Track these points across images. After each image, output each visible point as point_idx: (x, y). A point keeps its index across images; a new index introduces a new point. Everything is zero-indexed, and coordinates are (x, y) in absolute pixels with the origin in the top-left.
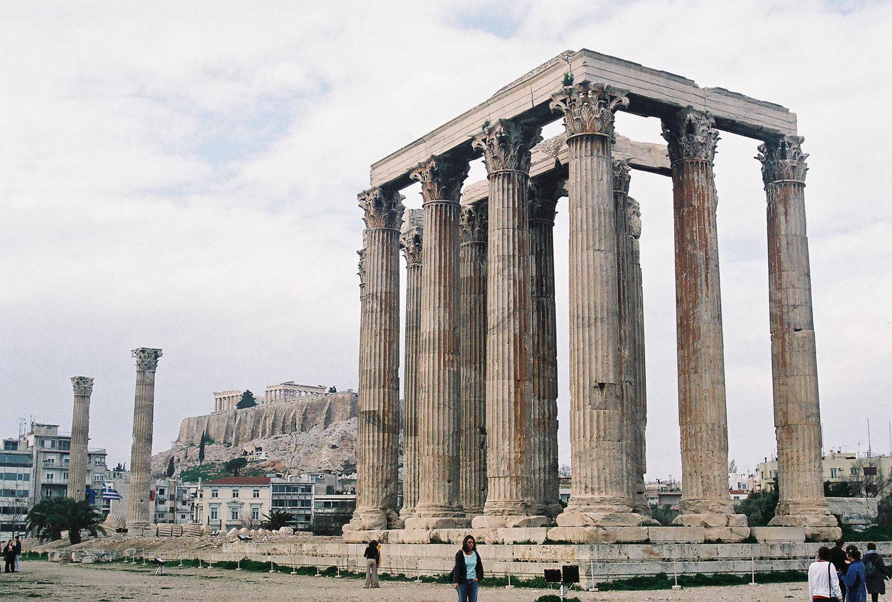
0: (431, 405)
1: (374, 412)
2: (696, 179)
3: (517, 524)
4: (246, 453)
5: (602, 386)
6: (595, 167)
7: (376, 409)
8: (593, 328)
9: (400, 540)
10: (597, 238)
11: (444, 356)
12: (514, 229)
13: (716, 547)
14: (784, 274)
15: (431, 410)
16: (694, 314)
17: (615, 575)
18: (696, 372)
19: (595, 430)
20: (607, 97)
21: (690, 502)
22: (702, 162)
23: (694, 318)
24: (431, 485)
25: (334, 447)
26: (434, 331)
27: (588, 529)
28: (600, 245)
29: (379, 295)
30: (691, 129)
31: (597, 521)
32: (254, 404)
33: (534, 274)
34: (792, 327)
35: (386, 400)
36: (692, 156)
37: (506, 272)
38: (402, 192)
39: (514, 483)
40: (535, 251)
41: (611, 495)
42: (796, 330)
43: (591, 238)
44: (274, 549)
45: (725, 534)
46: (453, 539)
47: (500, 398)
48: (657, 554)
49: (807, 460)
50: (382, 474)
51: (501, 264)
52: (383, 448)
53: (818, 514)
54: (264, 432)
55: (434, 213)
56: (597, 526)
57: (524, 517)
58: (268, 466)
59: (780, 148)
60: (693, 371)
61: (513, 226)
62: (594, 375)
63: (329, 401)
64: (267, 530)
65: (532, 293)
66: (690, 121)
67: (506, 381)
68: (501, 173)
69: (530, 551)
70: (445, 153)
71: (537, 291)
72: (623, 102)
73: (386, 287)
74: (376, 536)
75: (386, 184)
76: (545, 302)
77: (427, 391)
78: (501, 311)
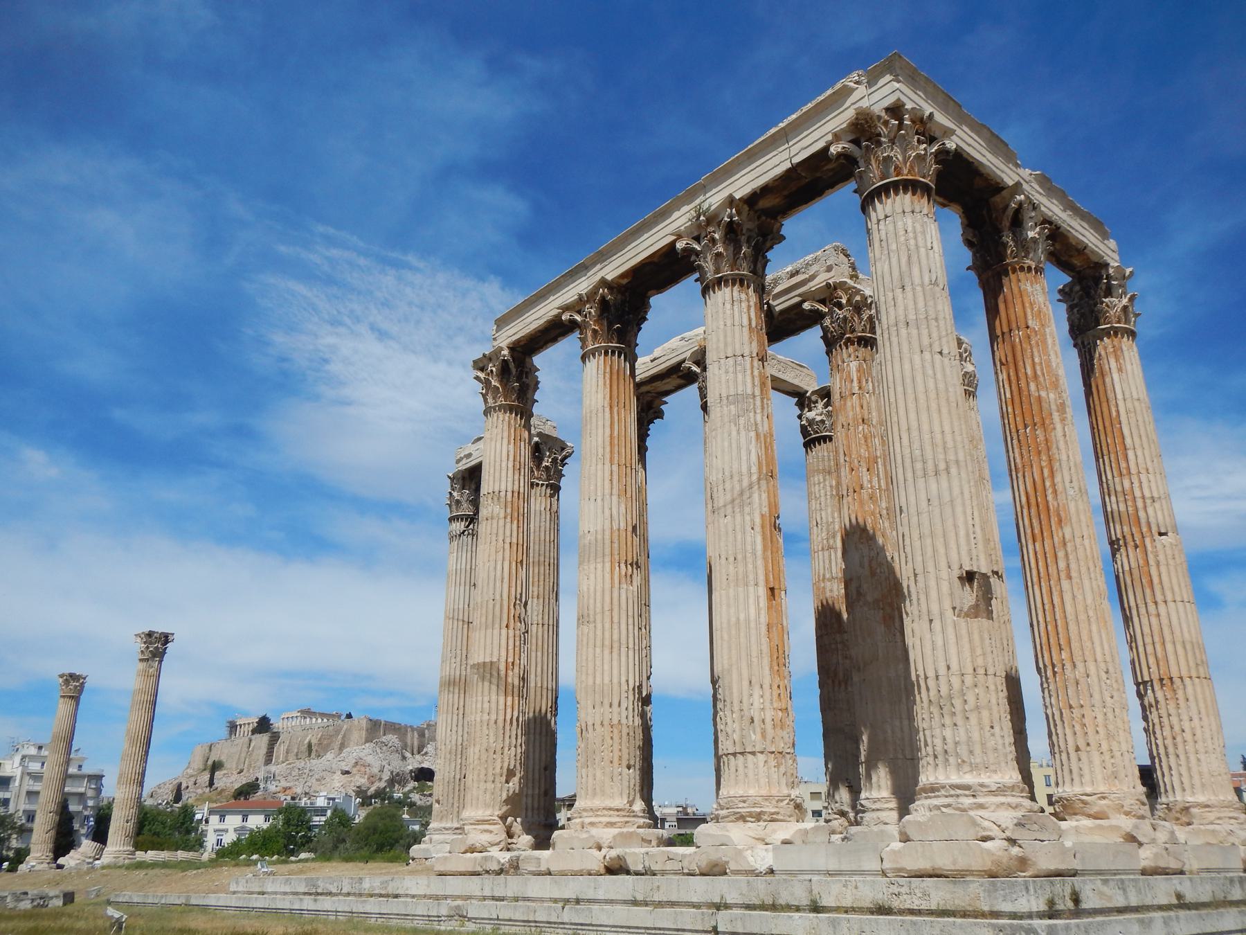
0: (599, 643)
2: (1029, 289)
4: (257, 779)
5: (969, 577)
6: (918, 227)
7: (495, 660)
8: (944, 477)
9: (543, 868)
14: (1131, 454)
15: (598, 650)
16: (1054, 485)
18: (1070, 578)
19: (967, 654)
20: (927, 135)
21: (1084, 798)
23: (1055, 492)
24: (599, 773)
25: (347, 772)
27: (988, 845)
28: (941, 345)
29: (503, 494)
30: (1017, 222)
31: (1007, 828)
34: (1154, 530)
35: (511, 647)
38: (538, 360)
39: (773, 763)
42: (1161, 534)
48: (1110, 898)
49: (1208, 735)
50: (502, 762)
53: (1242, 824)
54: (278, 757)
59: (1105, 281)
63: (345, 727)
67: (751, 589)
69: (854, 891)
70: (622, 276)
75: (518, 341)
78: (736, 478)
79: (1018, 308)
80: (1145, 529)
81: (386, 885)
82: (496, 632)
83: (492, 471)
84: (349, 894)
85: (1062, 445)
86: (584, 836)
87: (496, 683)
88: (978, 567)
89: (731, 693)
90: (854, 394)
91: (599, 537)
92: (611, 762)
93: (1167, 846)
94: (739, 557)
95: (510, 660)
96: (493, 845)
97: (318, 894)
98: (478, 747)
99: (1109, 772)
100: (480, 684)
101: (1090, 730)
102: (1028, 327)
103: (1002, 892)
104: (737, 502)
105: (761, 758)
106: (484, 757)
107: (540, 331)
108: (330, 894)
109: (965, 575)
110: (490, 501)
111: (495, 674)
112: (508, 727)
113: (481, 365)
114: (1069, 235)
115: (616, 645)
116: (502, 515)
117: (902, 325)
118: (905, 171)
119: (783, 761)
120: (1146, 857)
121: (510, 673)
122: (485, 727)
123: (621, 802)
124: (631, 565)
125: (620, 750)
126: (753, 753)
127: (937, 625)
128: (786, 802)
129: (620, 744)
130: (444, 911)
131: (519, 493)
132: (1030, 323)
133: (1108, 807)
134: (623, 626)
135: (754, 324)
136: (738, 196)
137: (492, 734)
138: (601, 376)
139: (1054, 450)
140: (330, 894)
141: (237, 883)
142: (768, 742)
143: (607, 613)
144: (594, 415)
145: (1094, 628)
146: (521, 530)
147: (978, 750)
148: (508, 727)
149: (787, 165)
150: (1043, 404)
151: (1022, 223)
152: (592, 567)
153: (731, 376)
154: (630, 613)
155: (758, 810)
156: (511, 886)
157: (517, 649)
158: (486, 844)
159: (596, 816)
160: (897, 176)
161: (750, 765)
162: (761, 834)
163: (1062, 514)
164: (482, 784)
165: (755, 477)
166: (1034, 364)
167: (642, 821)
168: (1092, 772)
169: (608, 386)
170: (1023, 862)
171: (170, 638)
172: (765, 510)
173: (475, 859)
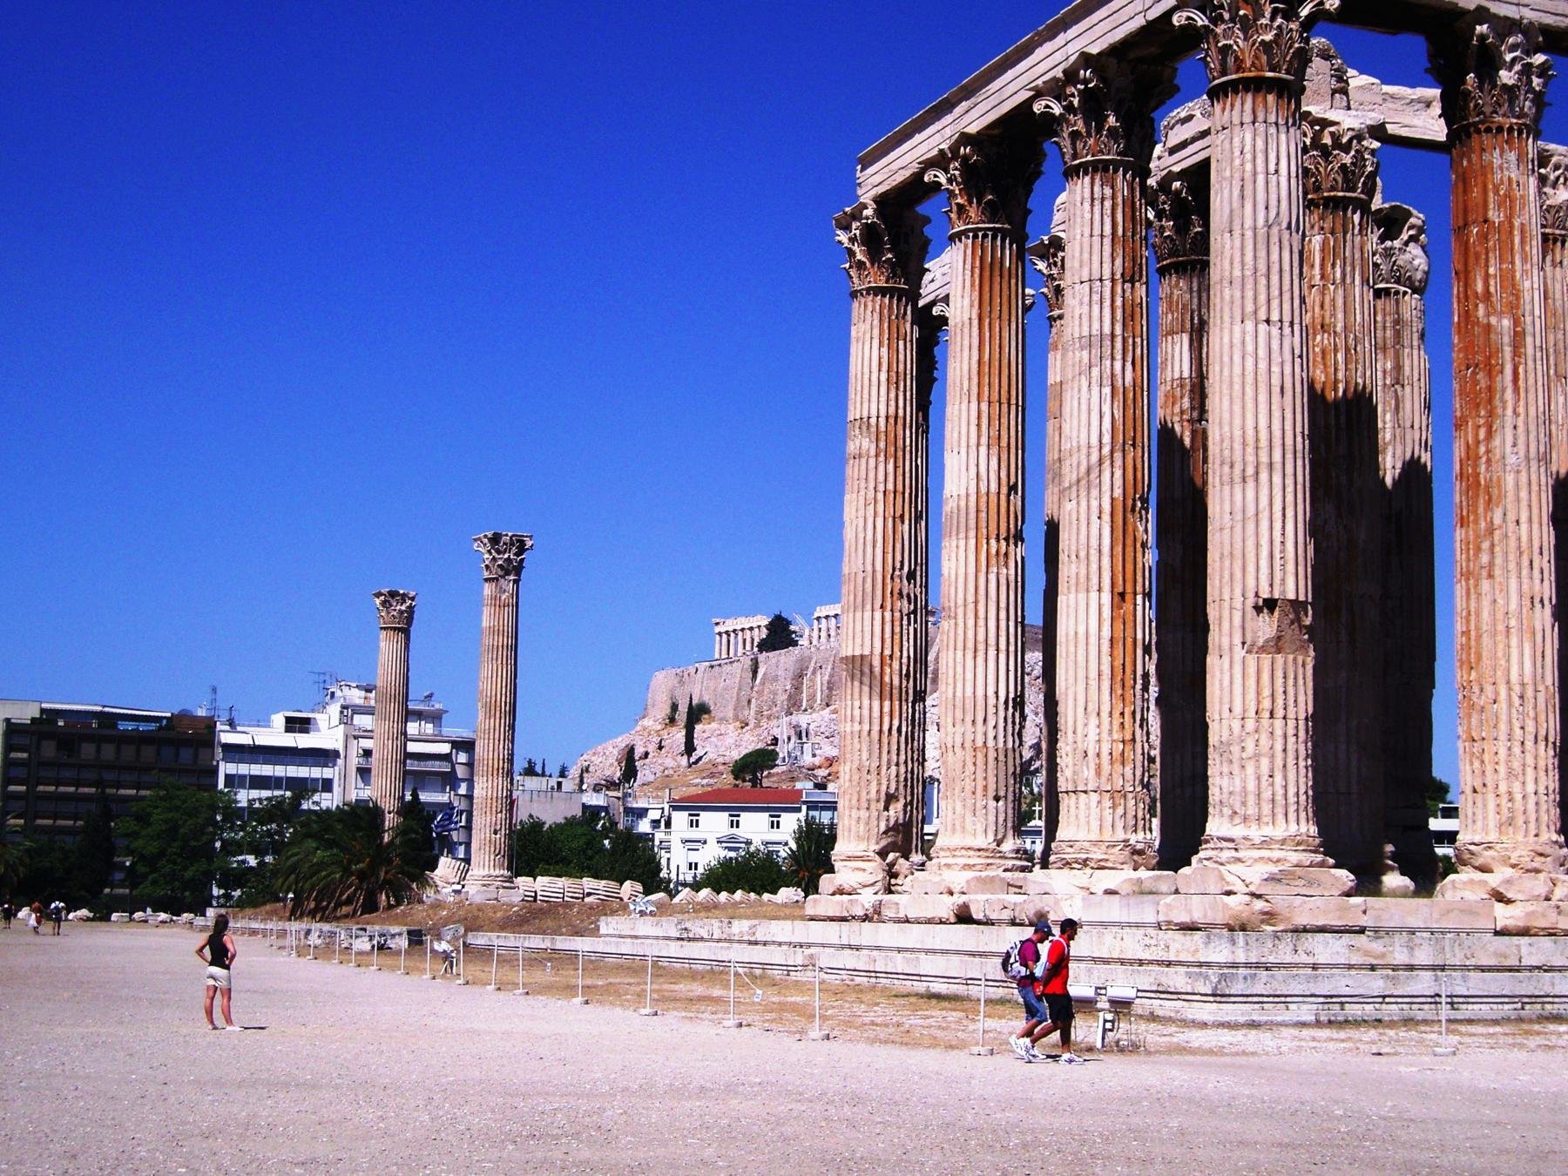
1: (862, 656)
2: (1497, 162)
3: (1112, 887)
5: (1270, 604)
7: (867, 652)
8: (1251, 485)
9: (901, 915)
10: (1262, 298)
11: (988, 543)
12: (1113, 280)
13: (1517, 943)
15: (959, 654)
17: (1278, 996)
18: (1490, 576)
19: (1252, 695)
21: (1472, 848)
23: (1489, 461)
24: (959, 806)
26: (967, 495)
29: (873, 421)
32: (795, 644)
33: (1186, 374)
37: (1095, 372)
40: (1188, 326)
41: (1286, 830)
43: (1249, 294)
44: (686, 929)
45: (1544, 916)
46: (993, 916)
47: (1082, 630)
48: (1383, 956)
50: (879, 784)
51: (1085, 353)
52: (881, 731)
54: (812, 698)
55: (969, 252)
56: (1253, 895)
57: (1128, 873)
58: (820, 767)
60: (1484, 573)
61: (1113, 274)
62: (1251, 583)
64: (752, 894)
65: (1182, 412)
67: (1094, 595)
71: (1192, 408)
74: (860, 907)
77: (952, 615)
78: (1084, 451)
79: (1476, 193)
81: (754, 930)
82: (868, 614)
83: (859, 388)
84: (719, 941)
86: (936, 879)
87: (868, 683)
88: (1284, 592)
89: (1066, 722)
90: (1313, 286)
91: (963, 504)
92: (974, 793)
93: (1560, 903)
94: (1083, 554)
95: (887, 652)
96: (865, 886)
97: (690, 940)
98: (848, 764)
99: (1504, 819)
100: (849, 684)
101: (1489, 769)
102: (1486, 221)
104: (1083, 482)
105: (1094, 797)
106: (856, 778)
107: (910, 183)
108: (702, 939)
109: (1261, 603)
110: (857, 431)
111: (867, 670)
112: (885, 740)
113: (844, 224)
115: (981, 647)
116: (873, 452)
117: (1226, 283)
119: (1122, 801)
120: (1505, 915)
121: (888, 670)
122: (856, 740)
123: (986, 841)
124: (1007, 539)
125: (985, 778)
126: (1085, 792)
127: (1226, 659)
128: (1119, 848)
130: (799, 961)
131: (896, 418)
133: (1493, 859)
135: (1120, 232)
136: (1094, 50)
137: (865, 749)
138: (968, 273)
139: (1497, 402)
140: (702, 939)
141: (607, 924)
142: (1104, 779)
143: (971, 607)
145: (1514, 641)
146: (900, 471)
147: (1251, 800)
148: (885, 740)
149: (1139, 22)
150: (1493, 336)
152: (954, 543)
153: (1086, 309)
154: (1003, 605)
155: (1084, 856)
156: (867, 934)
157: (897, 637)
158: (856, 885)
159: (954, 856)
160: (1237, 72)
161: (1082, 806)
162: (1085, 882)
163: (1495, 492)
164: (854, 812)
165: (1106, 450)
166: (1487, 276)
167: (1010, 863)
168: (1485, 818)
169: (977, 288)
170: (1270, 916)
171: (529, 543)
173: (842, 903)
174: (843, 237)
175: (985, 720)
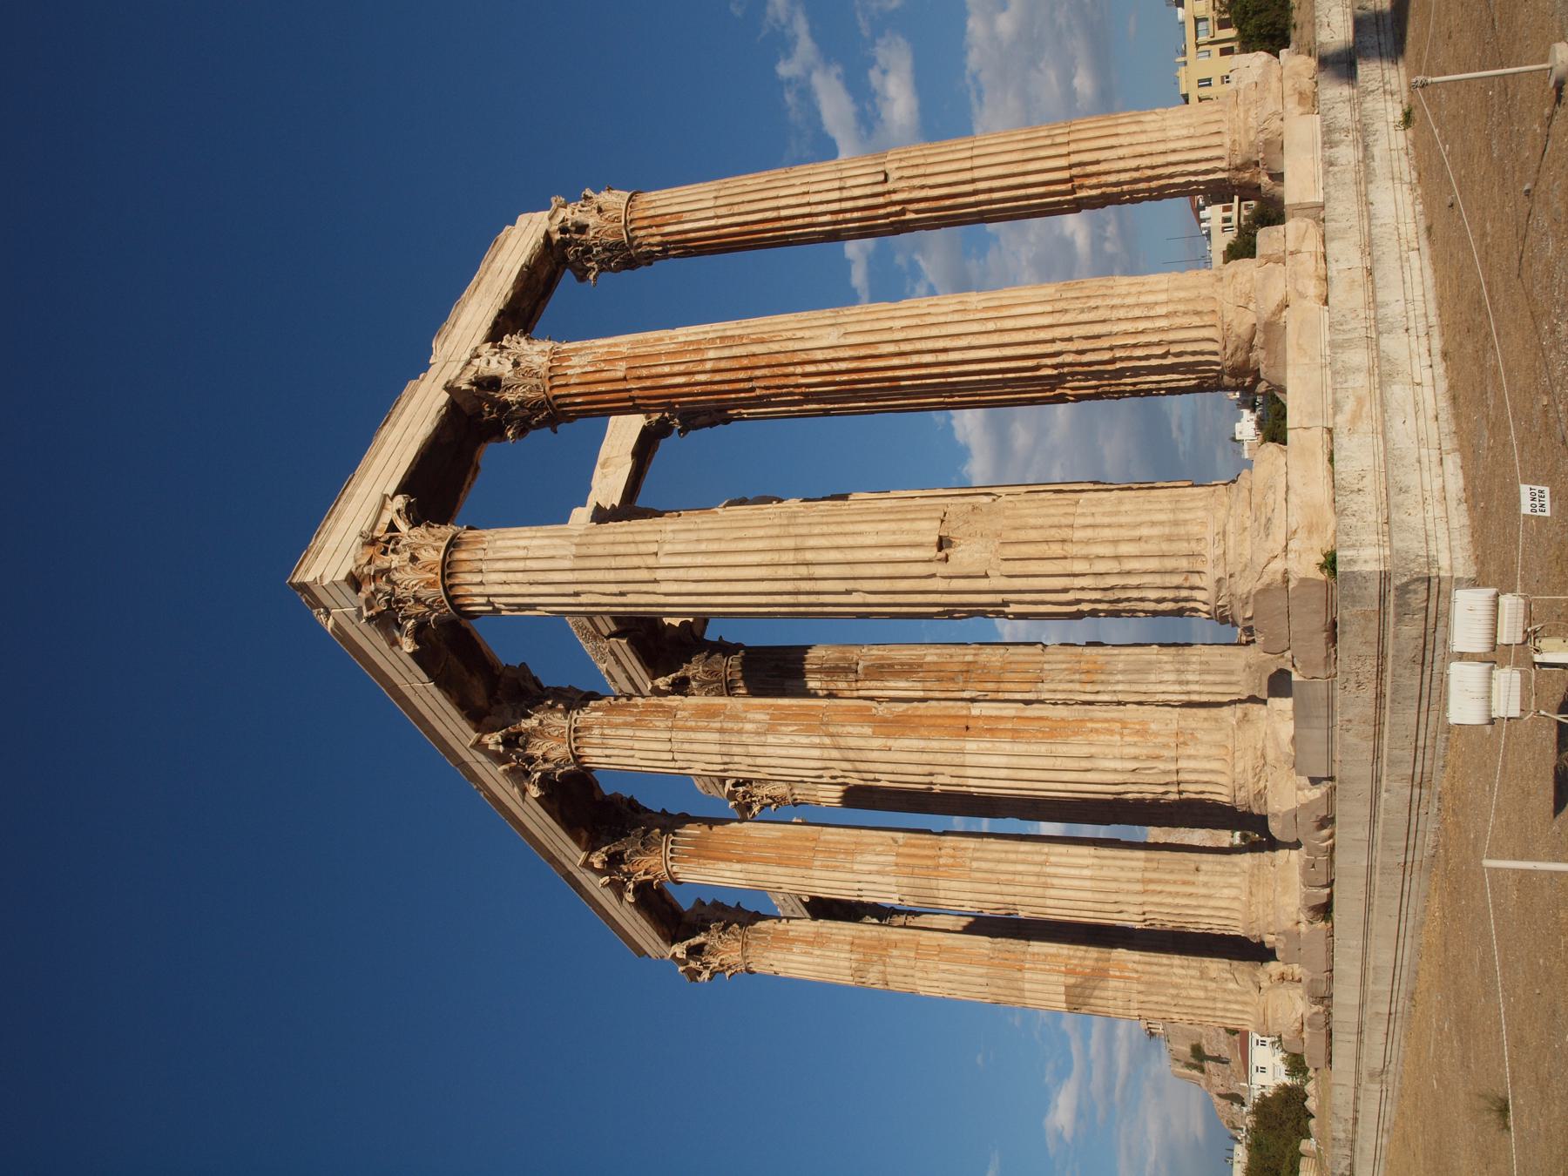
1: (1067, 995)
2: (579, 370)
5: (942, 543)
7: (1063, 989)
21: (1229, 352)
22: (551, 361)
36: (535, 381)
42: (886, 181)
50: (1190, 986)
66: (472, 383)
68: (573, 745)
70: (577, 840)
72: (400, 506)
73: (841, 951)
76: (867, 663)
80: (881, 200)
84: (1352, 1150)
85: (775, 347)
103: (1355, 590)
107: (650, 916)
109: (942, 555)
114: (510, 296)
115: (1043, 880)
116: (882, 968)
118: (431, 575)
129: (1167, 882)
132: (620, 374)
134: (1020, 868)
137: (1155, 998)
139: (783, 359)
140: (1351, 1165)
144: (751, 876)
151: (496, 377)
165: (827, 741)
172: (868, 731)
174: (706, 975)
175: (1115, 880)
